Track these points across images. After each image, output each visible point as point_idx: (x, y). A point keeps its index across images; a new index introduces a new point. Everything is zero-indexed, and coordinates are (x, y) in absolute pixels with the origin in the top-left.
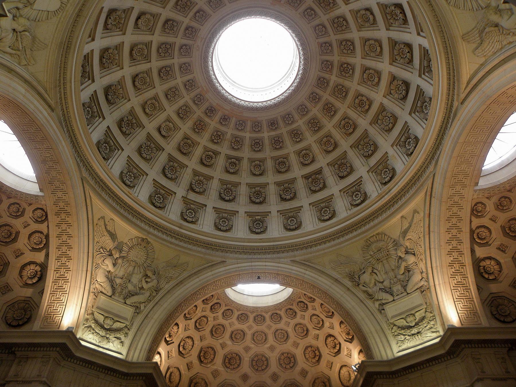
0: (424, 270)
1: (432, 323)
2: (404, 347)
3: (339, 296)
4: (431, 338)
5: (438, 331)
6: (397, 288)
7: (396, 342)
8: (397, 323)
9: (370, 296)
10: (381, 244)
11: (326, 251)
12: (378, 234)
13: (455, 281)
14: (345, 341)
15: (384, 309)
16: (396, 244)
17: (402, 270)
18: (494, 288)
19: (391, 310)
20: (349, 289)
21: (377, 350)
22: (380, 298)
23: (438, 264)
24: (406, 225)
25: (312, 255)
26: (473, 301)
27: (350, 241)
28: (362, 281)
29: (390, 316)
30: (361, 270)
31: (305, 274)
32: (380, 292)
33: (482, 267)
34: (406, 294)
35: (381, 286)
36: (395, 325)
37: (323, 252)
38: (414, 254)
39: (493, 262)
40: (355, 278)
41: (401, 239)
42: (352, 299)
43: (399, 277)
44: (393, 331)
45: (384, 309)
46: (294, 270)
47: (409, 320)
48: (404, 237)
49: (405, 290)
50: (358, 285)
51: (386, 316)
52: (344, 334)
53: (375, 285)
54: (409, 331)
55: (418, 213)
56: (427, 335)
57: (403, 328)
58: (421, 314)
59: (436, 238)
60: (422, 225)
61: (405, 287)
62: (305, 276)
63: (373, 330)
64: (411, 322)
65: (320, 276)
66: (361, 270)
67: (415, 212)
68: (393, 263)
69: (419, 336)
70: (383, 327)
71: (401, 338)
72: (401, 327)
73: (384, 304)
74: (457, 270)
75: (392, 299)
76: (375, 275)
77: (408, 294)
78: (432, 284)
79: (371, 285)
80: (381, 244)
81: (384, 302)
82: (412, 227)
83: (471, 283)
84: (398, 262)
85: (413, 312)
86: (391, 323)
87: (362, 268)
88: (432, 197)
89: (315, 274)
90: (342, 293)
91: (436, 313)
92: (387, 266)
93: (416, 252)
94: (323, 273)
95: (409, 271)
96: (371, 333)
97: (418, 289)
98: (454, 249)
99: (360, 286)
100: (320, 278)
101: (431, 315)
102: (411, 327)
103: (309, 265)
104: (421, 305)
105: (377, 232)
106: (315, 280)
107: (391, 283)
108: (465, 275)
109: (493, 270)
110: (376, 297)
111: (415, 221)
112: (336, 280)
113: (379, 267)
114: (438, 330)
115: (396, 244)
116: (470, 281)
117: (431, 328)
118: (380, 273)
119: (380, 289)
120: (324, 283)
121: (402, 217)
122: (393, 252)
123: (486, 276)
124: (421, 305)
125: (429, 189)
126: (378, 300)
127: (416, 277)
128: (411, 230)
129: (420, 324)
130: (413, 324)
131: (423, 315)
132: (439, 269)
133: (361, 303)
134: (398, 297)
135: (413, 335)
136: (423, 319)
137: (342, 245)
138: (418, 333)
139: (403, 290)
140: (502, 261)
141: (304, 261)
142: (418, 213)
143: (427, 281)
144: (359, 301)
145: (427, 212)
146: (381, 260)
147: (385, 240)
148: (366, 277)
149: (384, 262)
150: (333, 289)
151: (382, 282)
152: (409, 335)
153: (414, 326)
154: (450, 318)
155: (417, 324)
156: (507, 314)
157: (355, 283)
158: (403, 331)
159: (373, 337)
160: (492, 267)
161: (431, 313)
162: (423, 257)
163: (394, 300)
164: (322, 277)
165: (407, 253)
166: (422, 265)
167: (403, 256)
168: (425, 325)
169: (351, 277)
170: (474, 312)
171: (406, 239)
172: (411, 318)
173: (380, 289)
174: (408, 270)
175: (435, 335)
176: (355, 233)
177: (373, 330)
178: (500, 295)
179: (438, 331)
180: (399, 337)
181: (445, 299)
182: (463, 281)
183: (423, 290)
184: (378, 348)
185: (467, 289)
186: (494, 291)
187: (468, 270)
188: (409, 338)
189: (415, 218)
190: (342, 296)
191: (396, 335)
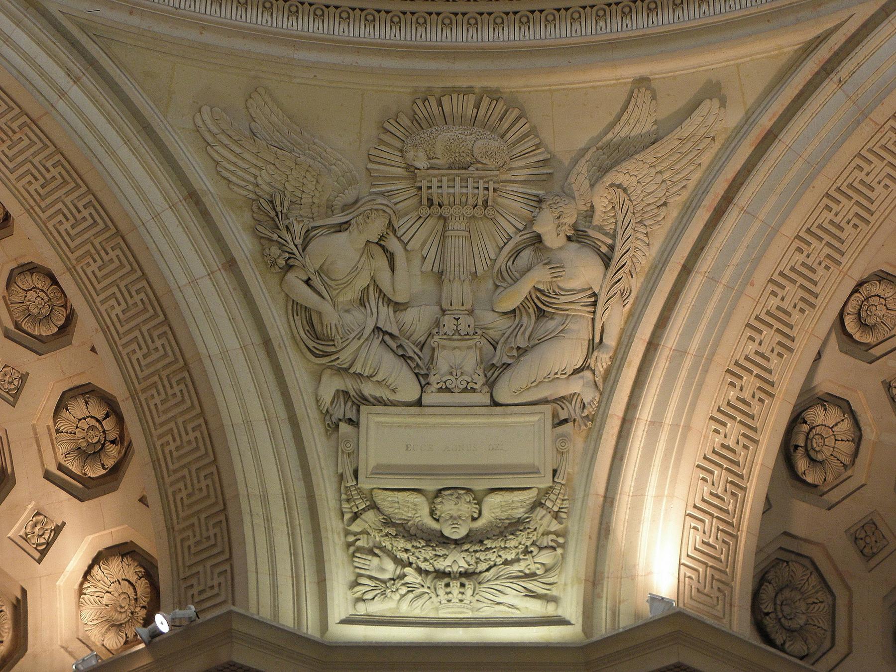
0: (611, 340)
1: (546, 558)
2: (378, 607)
3: (183, 280)
4: (516, 614)
5: (554, 600)
6: (458, 360)
7: (352, 578)
8: (386, 501)
9: (318, 341)
10: (484, 144)
11: (209, 38)
12: (495, 95)
13: (718, 440)
14: (48, 476)
15: (353, 423)
16: (547, 183)
17: (513, 298)
18: (805, 518)
19: (385, 439)
20: (231, 264)
21: (265, 580)
22: (357, 368)
23: (694, 347)
24: (640, 122)
25: (135, 20)
26: (736, 537)
27: (349, 59)
28: (313, 259)
29: (372, 464)
30: (330, 209)
31: (62, 94)
32: (377, 342)
33: (806, 428)
34: (487, 400)
35: (386, 317)
36: (374, 506)
37: (192, 34)
38: (607, 260)
39: (846, 425)
40: (281, 233)
41: (583, 167)
42: (232, 319)
43: (488, 318)
44: (354, 528)
45: (353, 423)
46: (17, 48)
47: (448, 507)
48: (604, 170)
49: (491, 384)
50: (290, 267)
51: (354, 454)
52: (61, 450)
53: (362, 302)
54: (429, 553)
55: (723, 104)
56: (501, 598)
57: (406, 531)
58: (510, 506)
59: (746, 241)
60: (706, 159)
61: (494, 372)
62: (61, 105)
63: (274, 488)
64: (455, 520)
65: (127, 142)
66: (330, 209)
67: (712, 91)
68: (489, 245)
69: (469, 592)
70: (319, 492)
71: (382, 570)
72: (394, 525)
73: (365, 400)
74: (744, 401)
75: (413, 396)
76: (382, 262)
77: (496, 404)
78: (618, 407)
79: (351, 294)
80: (484, 144)
81: (369, 390)
82: (661, 149)
83: (757, 469)
84: (516, 254)
85: (480, 485)
86: (360, 491)
87: (339, 202)
88: (834, 77)
89: (111, 121)
90: (199, 270)
91: (581, 530)
92: (457, 246)
93: (617, 254)
94: (147, 129)
95: (541, 314)
96: (265, 499)
97: (545, 401)
98: (780, 316)
99: (291, 276)
100: (124, 152)
101: (555, 526)
102: (445, 541)
103: (92, 63)
104: (533, 471)
105: (493, 84)
106: (100, 152)
107: (437, 323)
108: (755, 430)
109: (827, 452)
110: (345, 357)
111: (688, 128)
112: (194, 197)
113: (421, 234)
114: (554, 592)
115: (547, 183)
116: (759, 459)
117: (532, 576)
118: (409, 261)
119: (377, 329)
120: (136, 185)
121: (642, 82)
122: (513, 204)
123: (802, 464)
124: (533, 471)
125: (838, 40)
126: (343, 371)
127: (567, 353)
128: (649, 156)
129: (488, 543)
130: (462, 532)
131: (520, 513)
132: (688, 362)
133: (262, 353)
134: (445, 398)
135: (441, 574)
136: (513, 527)
137: (302, 55)
138: (466, 574)
139: (481, 380)
140: (869, 434)
141: (83, 28)
142: (723, 104)
143: (606, 385)
144: (257, 339)
145: (766, 122)
146: (445, 212)
147: (511, 137)
148: (341, 252)
149: (451, 224)
150: (166, 232)
151: (399, 307)
152: (419, 570)
153: (457, 543)
154: (641, 570)
155: (475, 539)
156: (794, 625)
157: (275, 251)
158: (401, 544)
159: (268, 519)
160: (830, 442)
161: (556, 516)
162: (636, 284)
163: (419, 403)
164: (134, 150)
165: (578, 236)
166: (614, 318)
167: (553, 239)
168: (510, 557)
169: (270, 217)
170: (723, 578)
171: (609, 178)
172: (465, 508)
173: (377, 329)
174: (541, 307)
175: (535, 608)
176: (386, 34)
177: (274, 488)
178: (806, 550)
179: (554, 600)
180: (376, 560)
181: (651, 490)
182: (739, 449)
183: (563, 415)
184: (273, 574)
185: (737, 486)
186: (798, 529)
187: (772, 418)
188: (419, 580)
189: (697, 117)
190: (194, 282)
191: (359, 550)
